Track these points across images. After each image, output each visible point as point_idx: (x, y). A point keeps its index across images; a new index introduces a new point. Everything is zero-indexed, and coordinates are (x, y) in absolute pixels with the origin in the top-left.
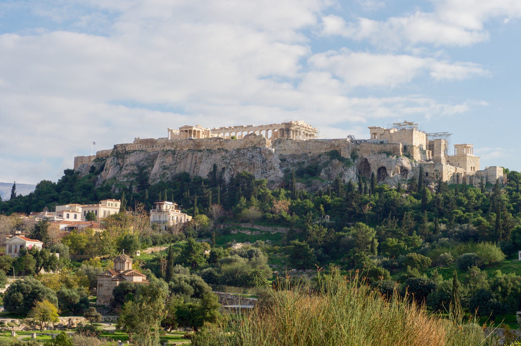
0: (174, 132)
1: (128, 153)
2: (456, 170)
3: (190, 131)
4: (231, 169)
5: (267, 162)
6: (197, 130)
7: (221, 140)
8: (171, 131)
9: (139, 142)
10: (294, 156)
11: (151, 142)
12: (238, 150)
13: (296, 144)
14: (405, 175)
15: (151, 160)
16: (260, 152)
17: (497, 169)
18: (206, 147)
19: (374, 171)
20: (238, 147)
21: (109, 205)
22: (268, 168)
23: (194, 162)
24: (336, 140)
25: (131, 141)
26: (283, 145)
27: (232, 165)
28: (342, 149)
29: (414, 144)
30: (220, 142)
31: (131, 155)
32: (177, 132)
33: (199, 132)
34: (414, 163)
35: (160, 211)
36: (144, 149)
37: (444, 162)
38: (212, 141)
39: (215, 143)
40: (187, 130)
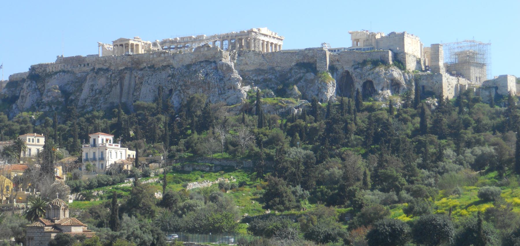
0: (106, 46)
1: (50, 75)
2: (458, 81)
3: (127, 45)
4: (180, 91)
5: (225, 79)
6: (135, 43)
7: (166, 55)
8: (103, 46)
9: (62, 60)
10: (259, 71)
11: (78, 60)
12: (188, 66)
13: (260, 57)
14: (397, 89)
15: (80, 82)
16: (216, 68)
17: (509, 78)
18: (147, 64)
19: (358, 86)
20: (187, 63)
21: (29, 141)
22: (226, 89)
23: (133, 83)
24: (310, 49)
25: (52, 60)
27: (181, 86)
28: (317, 61)
29: (406, 51)
30: (165, 57)
31: (53, 77)
32: (109, 46)
33: (137, 45)
34: (406, 75)
35: (95, 145)
36: (70, 69)
37: (443, 71)
38: (155, 56)
39: (159, 59)
40: (122, 44)
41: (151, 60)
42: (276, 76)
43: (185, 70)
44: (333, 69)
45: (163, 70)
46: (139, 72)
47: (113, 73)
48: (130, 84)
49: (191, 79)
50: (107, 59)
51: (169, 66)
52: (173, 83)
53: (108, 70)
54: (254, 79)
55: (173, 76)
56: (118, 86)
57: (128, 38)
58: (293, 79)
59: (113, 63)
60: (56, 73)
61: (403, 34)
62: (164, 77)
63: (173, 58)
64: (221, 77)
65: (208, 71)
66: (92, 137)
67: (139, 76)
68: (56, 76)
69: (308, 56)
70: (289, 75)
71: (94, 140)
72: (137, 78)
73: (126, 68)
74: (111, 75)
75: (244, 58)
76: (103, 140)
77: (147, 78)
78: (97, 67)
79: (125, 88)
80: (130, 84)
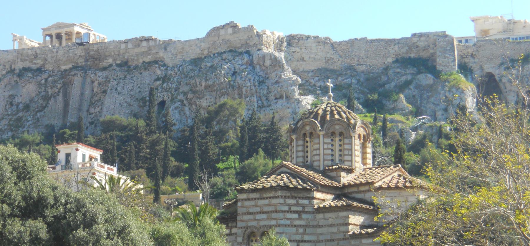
4: (182, 101)
5: (269, 82)
7: (151, 43)
8: (21, 39)
10: (325, 73)
12: (196, 62)
13: (328, 47)
16: (251, 63)
18: (114, 60)
20: (193, 56)
22: (272, 98)
23: (88, 92)
24: (421, 35)
27: (185, 94)
28: (438, 53)
30: (149, 48)
38: (130, 46)
39: (137, 50)
41: (121, 52)
42: (359, 81)
43: (190, 67)
44: (464, 69)
45: (145, 69)
46: (100, 74)
47: (50, 76)
48: (82, 94)
49: (206, 81)
50: (38, 52)
51: (156, 62)
52: (168, 90)
53: (40, 71)
54: (318, 84)
55: (165, 79)
56: (60, 98)
57: (70, 22)
58: (393, 84)
59: (49, 60)
62: (147, 82)
63: (165, 49)
64: (261, 79)
65: (237, 67)
67: (100, 79)
69: (418, 46)
70: (384, 78)
71: (68, 156)
72: (96, 83)
73: (75, 68)
74: (46, 80)
75: (298, 49)
76: (84, 156)
77: (116, 82)
78: (19, 66)
79: (74, 101)
80: (82, 94)
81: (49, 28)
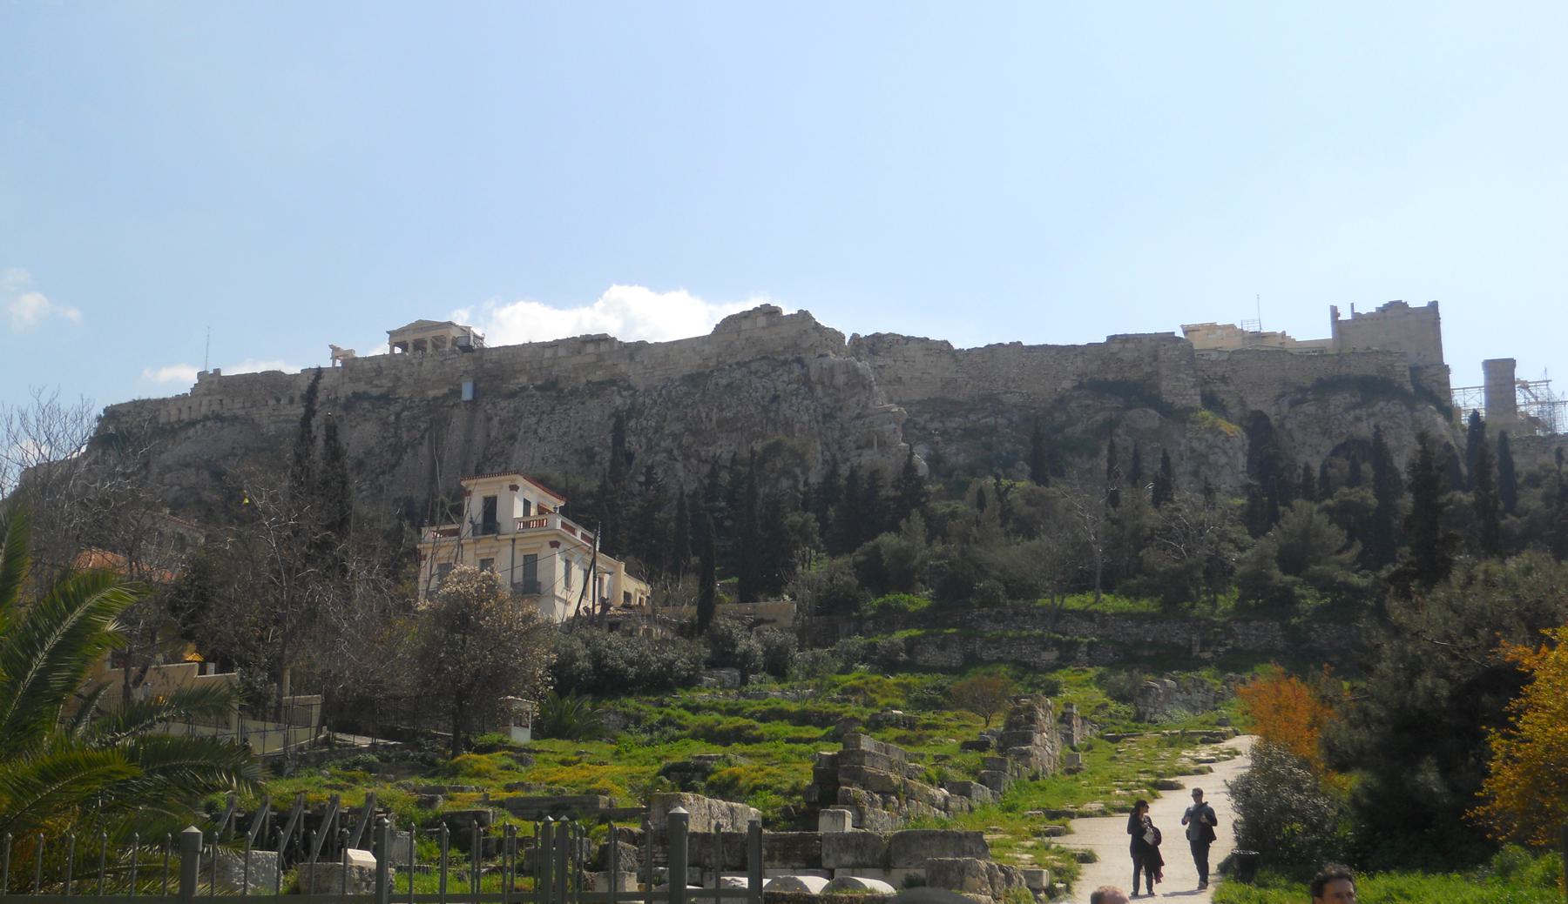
4: (670, 452)
7: (603, 347)
12: (693, 379)
16: (806, 380)
18: (532, 379)
20: (686, 371)
23: (479, 437)
26: (890, 362)
27: (676, 437)
30: (600, 357)
36: (241, 413)
41: (545, 363)
42: (1010, 421)
43: (684, 389)
45: (592, 395)
46: (503, 404)
47: (405, 408)
51: (612, 382)
53: (385, 399)
56: (424, 449)
58: (1080, 428)
60: (193, 423)
61: (1434, 306)
62: (596, 418)
63: (632, 357)
65: (780, 386)
66: (478, 492)
67: (504, 414)
68: (191, 432)
69: (1120, 360)
70: (1060, 417)
71: (490, 505)
72: (496, 421)
74: (398, 416)
77: (534, 420)
81: (402, 331)
